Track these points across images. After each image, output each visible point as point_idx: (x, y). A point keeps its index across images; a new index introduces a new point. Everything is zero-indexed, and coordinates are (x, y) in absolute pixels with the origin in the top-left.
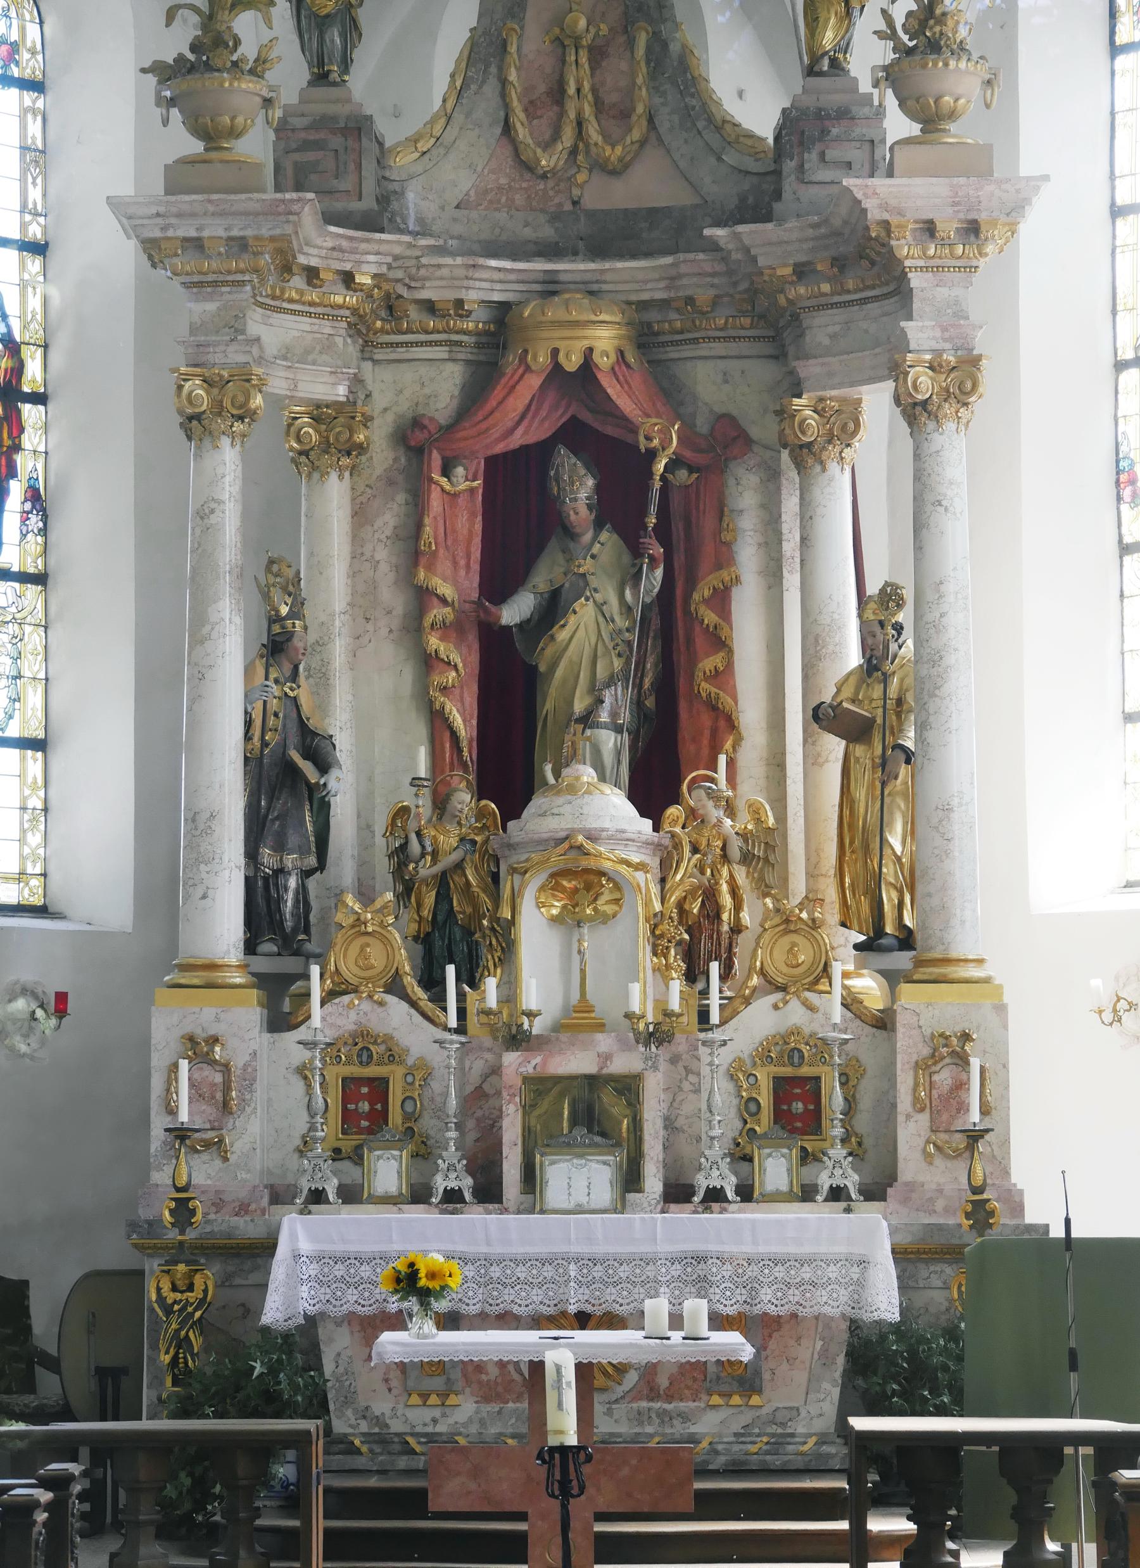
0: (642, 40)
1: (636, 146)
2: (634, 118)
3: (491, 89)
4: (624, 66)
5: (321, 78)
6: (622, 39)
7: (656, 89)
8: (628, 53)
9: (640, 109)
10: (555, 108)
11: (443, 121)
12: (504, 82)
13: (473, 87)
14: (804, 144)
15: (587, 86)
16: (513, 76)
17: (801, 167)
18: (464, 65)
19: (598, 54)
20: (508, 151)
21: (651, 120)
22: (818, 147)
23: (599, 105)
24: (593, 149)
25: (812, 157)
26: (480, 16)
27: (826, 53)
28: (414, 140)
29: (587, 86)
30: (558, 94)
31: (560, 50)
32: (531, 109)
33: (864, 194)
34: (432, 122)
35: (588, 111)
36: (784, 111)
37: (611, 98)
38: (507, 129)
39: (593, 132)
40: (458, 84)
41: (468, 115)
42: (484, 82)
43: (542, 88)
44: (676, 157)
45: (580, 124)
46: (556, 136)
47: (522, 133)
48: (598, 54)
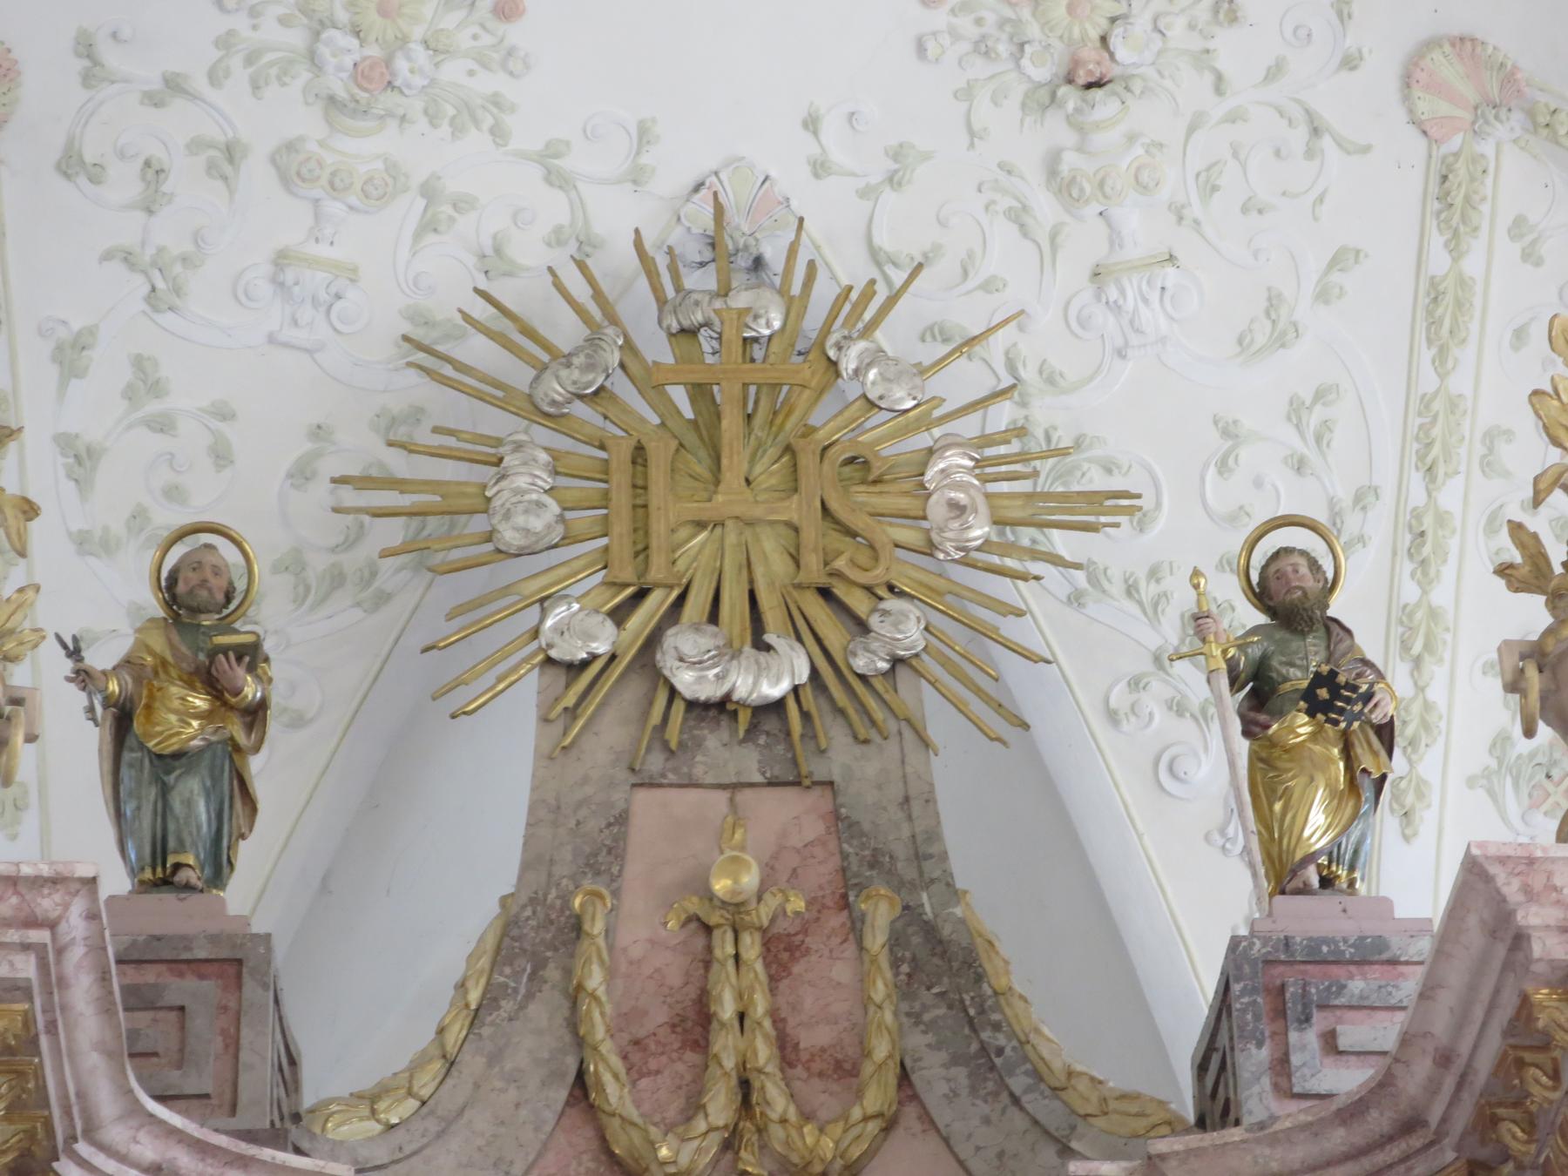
0: (880, 914)
1: (873, 1127)
2: (868, 1069)
3: (545, 1012)
4: (842, 972)
5: (160, 873)
6: (837, 920)
7: (916, 1018)
8: (850, 949)
9: (881, 1049)
10: (691, 1057)
11: (437, 1066)
12: (575, 995)
13: (507, 1006)
14: (1284, 1010)
15: (760, 1005)
16: (595, 980)
17: (1282, 1065)
18: (484, 962)
19: (783, 951)
20: (584, 1137)
21: (904, 1077)
22: (1320, 1021)
23: (786, 1048)
24: (777, 1132)
25: (1305, 1043)
26: (526, 867)
27: (1310, 858)
28: (371, 1099)
29: (760, 1005)
30: (696, 1024)
31: (699, 942)
32: (636, 1052)
33: (1527, 890)
34: (414, 1068)
35: (764, 1053)
36: (1235, 942)
37: (812, 1038)
38: (582, 1085)
39: (775, 1099)
40: (474, 996)
41: (494, 1059)
42: (530, 996)
43: (659, 1016)
44: (964, 1151)
45: (745, 1085)
46: (695, 1106)
47: (614, 1092)
48: (783, 951)
